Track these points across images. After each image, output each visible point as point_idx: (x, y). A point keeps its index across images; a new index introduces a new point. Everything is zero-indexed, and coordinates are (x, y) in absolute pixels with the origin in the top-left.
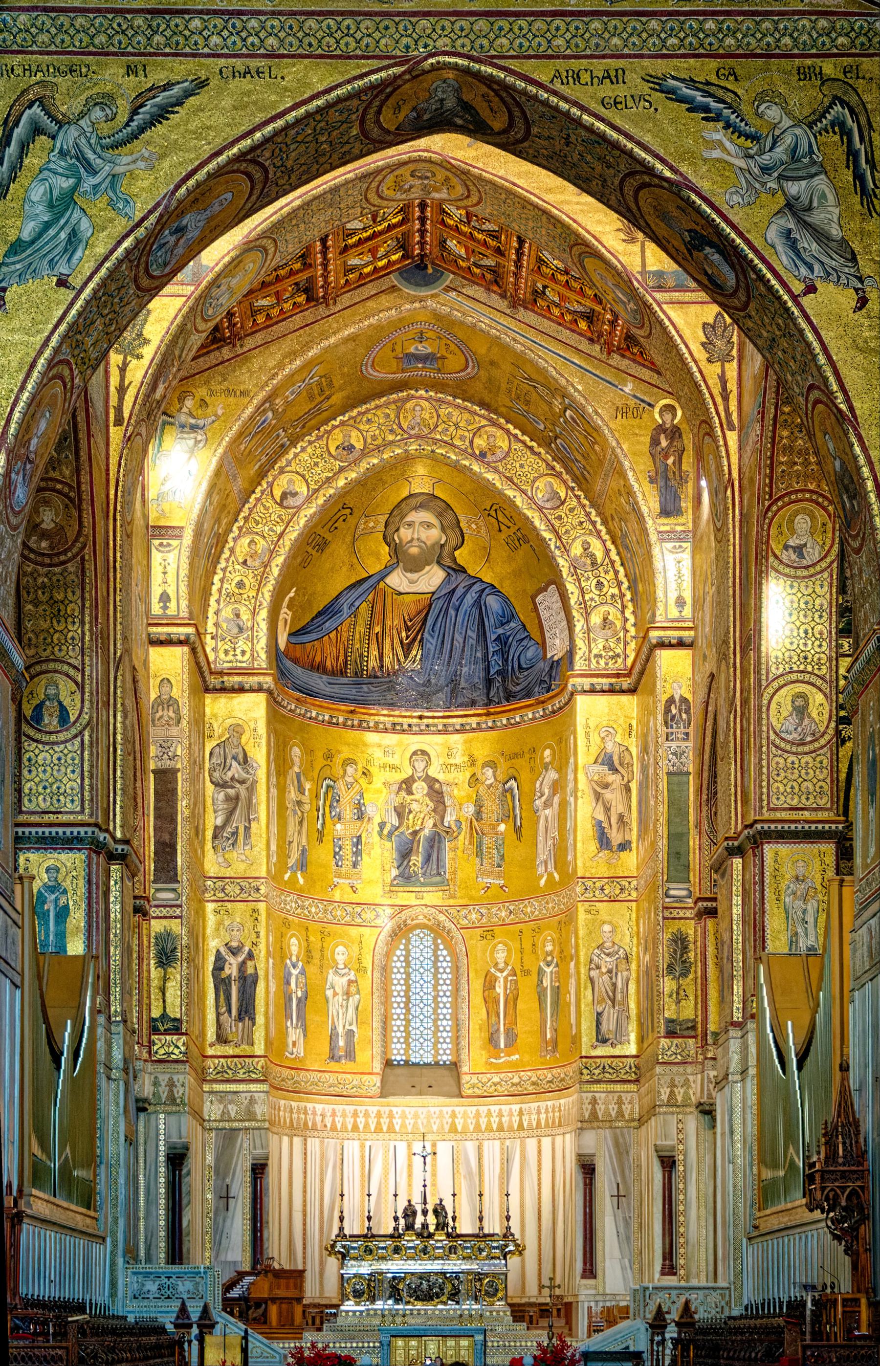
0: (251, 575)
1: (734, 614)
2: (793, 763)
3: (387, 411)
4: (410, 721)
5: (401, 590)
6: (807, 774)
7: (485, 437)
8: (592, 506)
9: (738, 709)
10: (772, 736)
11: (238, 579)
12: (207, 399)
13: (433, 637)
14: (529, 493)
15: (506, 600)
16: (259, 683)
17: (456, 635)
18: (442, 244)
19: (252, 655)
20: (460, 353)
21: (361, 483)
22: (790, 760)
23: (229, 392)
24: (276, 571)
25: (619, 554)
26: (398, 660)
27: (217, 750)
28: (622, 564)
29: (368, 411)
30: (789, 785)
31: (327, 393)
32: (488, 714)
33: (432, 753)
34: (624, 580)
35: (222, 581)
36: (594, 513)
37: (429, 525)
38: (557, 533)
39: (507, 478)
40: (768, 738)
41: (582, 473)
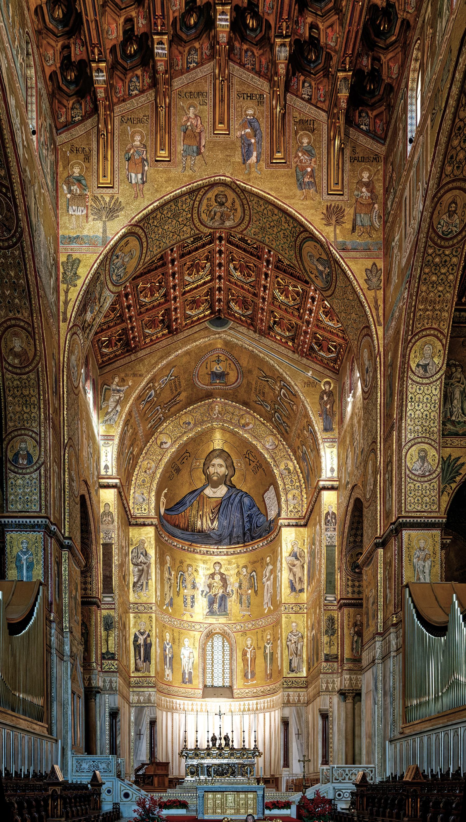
1: (380, 422)
2: (419, 487)
6: (426, 493)
9: (382, 472)
10: (408, 472)
12: (125, 378)
18: (229, 308)
20: (235, 369)
21: (193, 440)
22: (417, 485)
23: (135, 375)
29: (196, 408)
30: (416, 499)
31: (179, 390)
33: (222, 563)
40: (405, 473)
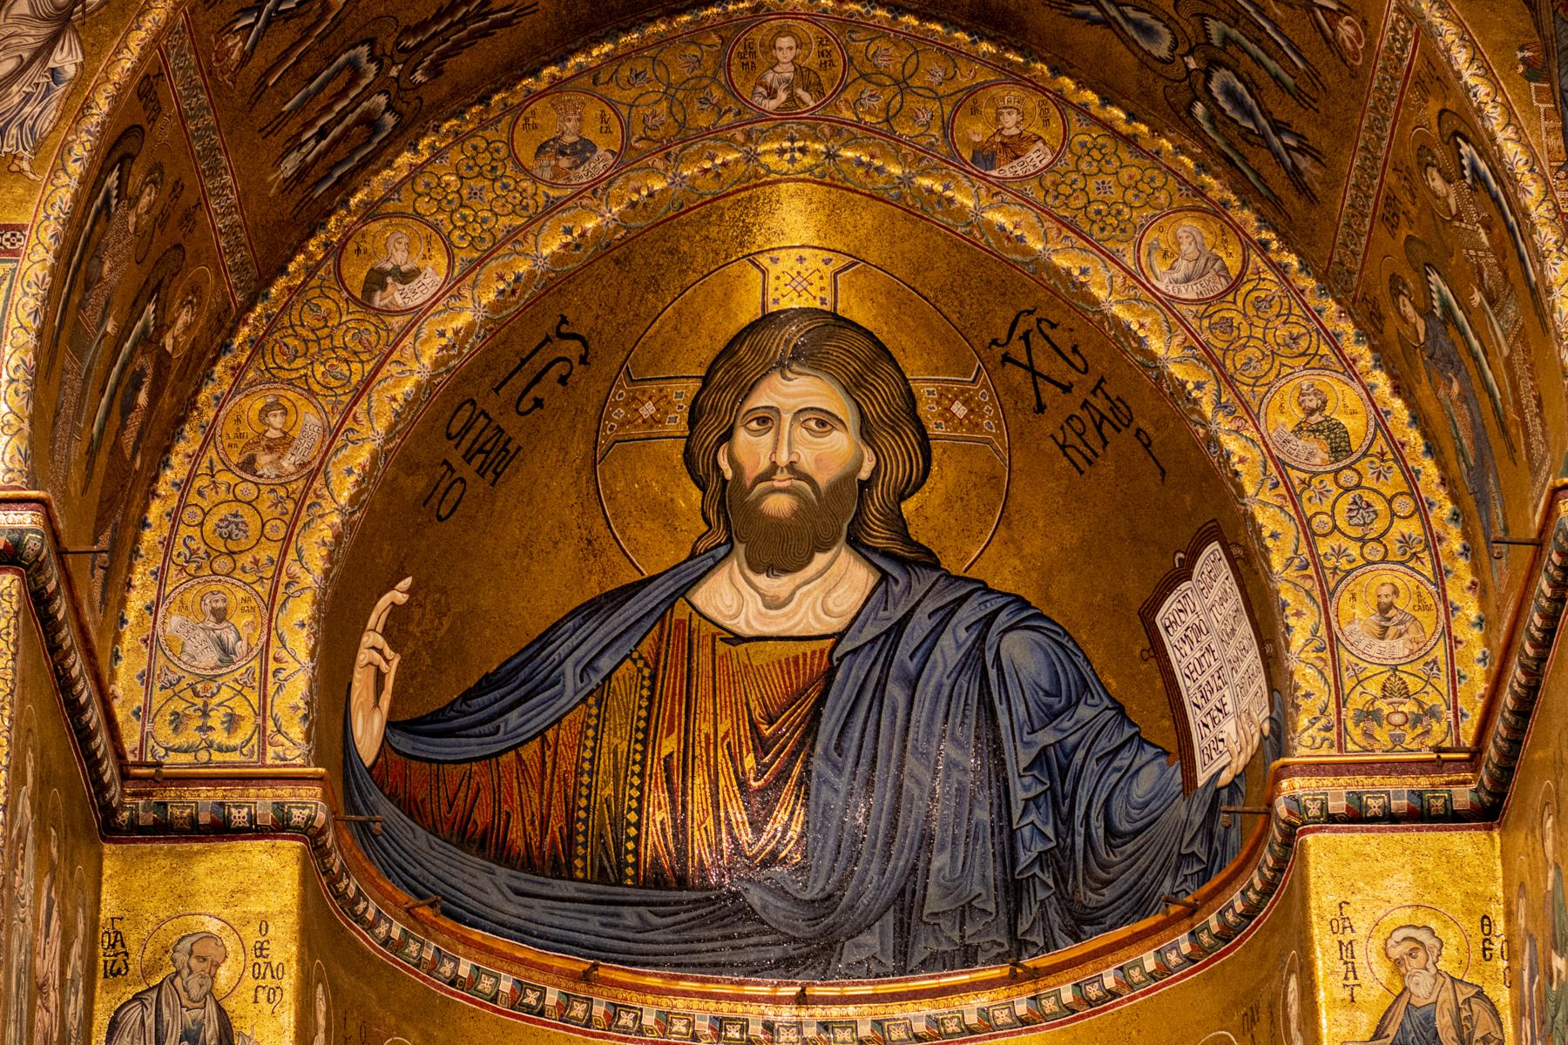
0: (267, 498)
3: (693, 51)
4: (770, 1012)
5: (741, 626)
7: (991, 111)
8: (1331, 281)
11: (224, 511)
13: (839, 770)
14: (1129, 261)
15: (1062, 641)
16: (279, 806)
17: (911, 762)
19: (260, 729)
24: (344, 491)
25: (1418, 419)
26: (734, 840)
27: (135, 1013)
28: (1429, 451)
32: (1013, 980)
34: (1440, 495)
35: (175, 517)
36: (1331, 306)
37: (825, 421)
38: (1220, 366)
39: (1059, 220)
41: (1295, 173)
